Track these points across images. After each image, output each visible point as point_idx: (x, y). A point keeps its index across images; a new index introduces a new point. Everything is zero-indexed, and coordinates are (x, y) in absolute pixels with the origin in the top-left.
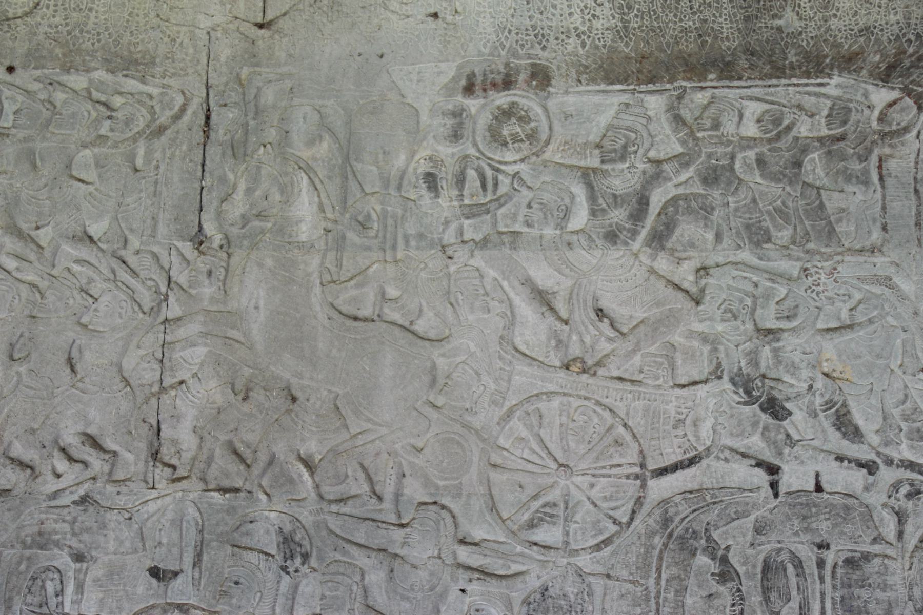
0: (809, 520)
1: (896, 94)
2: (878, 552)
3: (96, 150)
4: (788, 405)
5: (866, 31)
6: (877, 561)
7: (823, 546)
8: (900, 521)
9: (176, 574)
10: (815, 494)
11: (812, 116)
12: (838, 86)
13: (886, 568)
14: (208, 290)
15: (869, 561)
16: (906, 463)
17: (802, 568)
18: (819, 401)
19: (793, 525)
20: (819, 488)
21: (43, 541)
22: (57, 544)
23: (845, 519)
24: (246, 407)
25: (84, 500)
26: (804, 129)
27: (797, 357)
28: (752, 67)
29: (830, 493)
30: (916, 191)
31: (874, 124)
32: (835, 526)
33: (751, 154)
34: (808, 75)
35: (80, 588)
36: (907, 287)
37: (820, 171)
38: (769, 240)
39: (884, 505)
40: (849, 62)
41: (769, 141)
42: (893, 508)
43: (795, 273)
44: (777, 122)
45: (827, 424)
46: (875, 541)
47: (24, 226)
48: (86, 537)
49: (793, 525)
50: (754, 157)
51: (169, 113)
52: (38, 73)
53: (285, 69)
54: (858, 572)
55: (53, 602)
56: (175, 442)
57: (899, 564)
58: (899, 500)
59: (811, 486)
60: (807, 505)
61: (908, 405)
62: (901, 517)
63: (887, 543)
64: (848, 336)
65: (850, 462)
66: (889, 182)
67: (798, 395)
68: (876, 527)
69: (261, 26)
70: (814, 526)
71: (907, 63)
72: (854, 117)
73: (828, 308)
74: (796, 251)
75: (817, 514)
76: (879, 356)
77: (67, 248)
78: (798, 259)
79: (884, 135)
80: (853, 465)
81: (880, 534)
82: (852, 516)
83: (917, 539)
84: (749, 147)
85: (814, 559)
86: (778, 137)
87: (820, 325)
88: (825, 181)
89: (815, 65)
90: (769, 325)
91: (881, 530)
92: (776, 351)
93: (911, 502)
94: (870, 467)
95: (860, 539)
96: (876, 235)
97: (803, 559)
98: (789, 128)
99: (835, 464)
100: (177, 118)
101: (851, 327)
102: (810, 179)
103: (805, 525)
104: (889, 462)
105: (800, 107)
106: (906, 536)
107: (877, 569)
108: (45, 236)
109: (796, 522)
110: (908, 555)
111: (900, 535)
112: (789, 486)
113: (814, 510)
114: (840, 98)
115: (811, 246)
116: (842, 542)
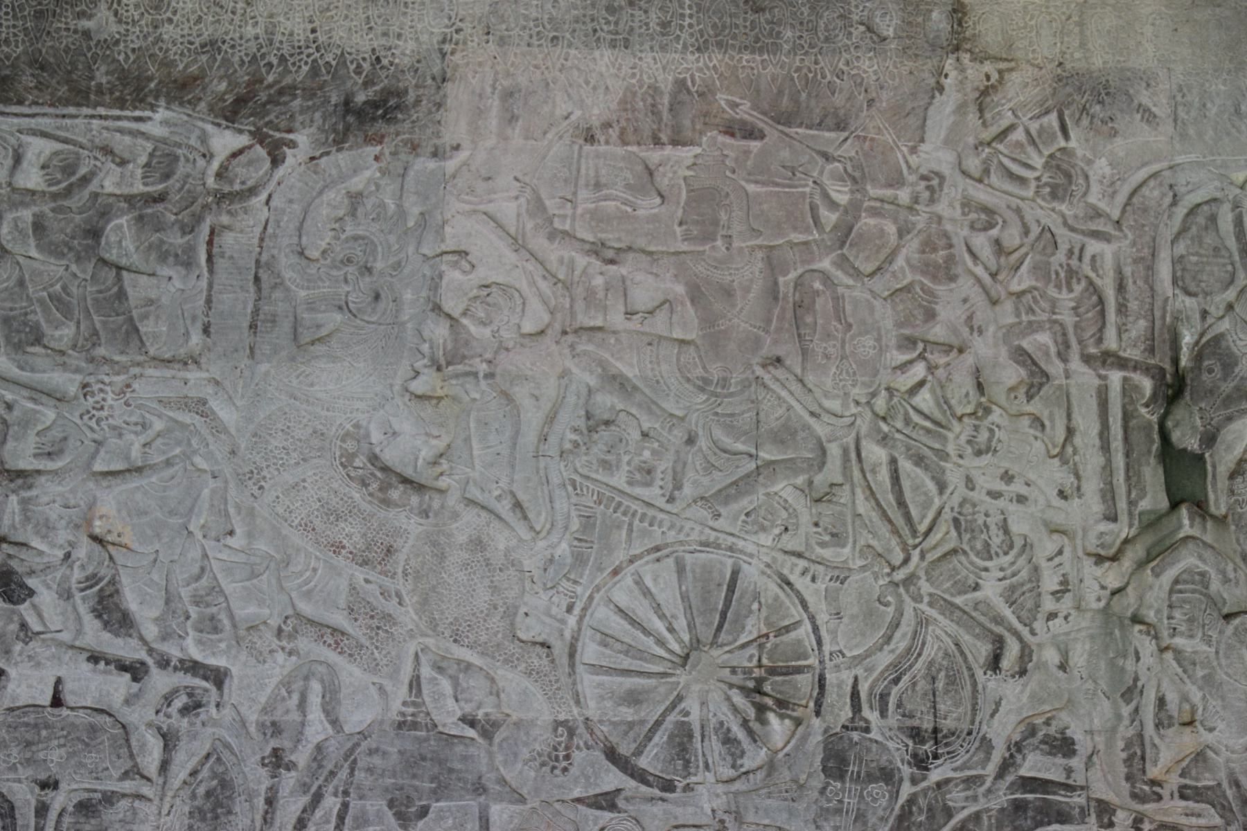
0: (34, 748)
1: (244, 140)
2: (128, 791)
4: (31, 582)
5: (212, 45)
6: (124, 804)
7: (49, 784)
8: (166, 746)
10: (49, 709)
11: (123, 163)
12: (165, 123)
13: (135, 814)
15: (112, 804)
16: (188, 664)
17: (13, 817)
18: (77, 574)
19: (9, 755)
20: (57, 702)
23: (87, 745)
26: (110, 182)
27: (54, 512)
28: (40, 86)
29: (72, 709)
30: (257, 279)
31: (211, 181)
32: (71, 755)
33: (27, 215)
34: (121, 103)
36: (226, 414)
37: (129, 244)
38: (38, 341)
39: (149, 725)
40: (182, 89)
41: (55, 196)
42: (159, 729)
43: (73, 389)
44: (69, 169)
45: (83, 609)
46: (126, 775)
49: (9, 755)
50: (30, 219)
54: (93, 821)
57: (154, 808)
58: (169, 716)
59: (46, 699)
60: (36, 725)
61: (204, 582)
62: (169, 740)
63: (143, 777)
64: (135, 482)
65: (107, 664)
66: (220, 264)
67: (48, 567)
68: (132, 756)
70: (41, 755)
71: (263, 96)
72: (182, 169)
73: (113, 442)
74: (75, 359)
75: (49, 739)
76: (172, 513)
78: (77, 370)
79: (221, 197)
80: (112, 667)
81: (136, 765)
82: (98, 741)
83: (188, 771)
84: (23, 204)
85: (33, 803)
86: (68, 192)
87: (98, 467)
88: (136, 260)
89: (133, 90)
90: (22, 465)
91: (139, 760)
92: (24, 502)
93: (186, 720)
94: (136, 671)
95: (106, 773)
96: (196, 338)
97: (17, 804)
98: (85, 180)
99: (86, 667)
101: (139, 470)
102: (112, 255)
103: (28, 755)
104: (164, 663)
105: (107, 151)
106: (174, 768)
107: (121, 816)
109: (15, 751)
110: (170, 794)
111: (164, 766)
112: (14, 699)
113: (44, 733)
114: (164, 141)
115: (101, 351)
116: (77, 778)
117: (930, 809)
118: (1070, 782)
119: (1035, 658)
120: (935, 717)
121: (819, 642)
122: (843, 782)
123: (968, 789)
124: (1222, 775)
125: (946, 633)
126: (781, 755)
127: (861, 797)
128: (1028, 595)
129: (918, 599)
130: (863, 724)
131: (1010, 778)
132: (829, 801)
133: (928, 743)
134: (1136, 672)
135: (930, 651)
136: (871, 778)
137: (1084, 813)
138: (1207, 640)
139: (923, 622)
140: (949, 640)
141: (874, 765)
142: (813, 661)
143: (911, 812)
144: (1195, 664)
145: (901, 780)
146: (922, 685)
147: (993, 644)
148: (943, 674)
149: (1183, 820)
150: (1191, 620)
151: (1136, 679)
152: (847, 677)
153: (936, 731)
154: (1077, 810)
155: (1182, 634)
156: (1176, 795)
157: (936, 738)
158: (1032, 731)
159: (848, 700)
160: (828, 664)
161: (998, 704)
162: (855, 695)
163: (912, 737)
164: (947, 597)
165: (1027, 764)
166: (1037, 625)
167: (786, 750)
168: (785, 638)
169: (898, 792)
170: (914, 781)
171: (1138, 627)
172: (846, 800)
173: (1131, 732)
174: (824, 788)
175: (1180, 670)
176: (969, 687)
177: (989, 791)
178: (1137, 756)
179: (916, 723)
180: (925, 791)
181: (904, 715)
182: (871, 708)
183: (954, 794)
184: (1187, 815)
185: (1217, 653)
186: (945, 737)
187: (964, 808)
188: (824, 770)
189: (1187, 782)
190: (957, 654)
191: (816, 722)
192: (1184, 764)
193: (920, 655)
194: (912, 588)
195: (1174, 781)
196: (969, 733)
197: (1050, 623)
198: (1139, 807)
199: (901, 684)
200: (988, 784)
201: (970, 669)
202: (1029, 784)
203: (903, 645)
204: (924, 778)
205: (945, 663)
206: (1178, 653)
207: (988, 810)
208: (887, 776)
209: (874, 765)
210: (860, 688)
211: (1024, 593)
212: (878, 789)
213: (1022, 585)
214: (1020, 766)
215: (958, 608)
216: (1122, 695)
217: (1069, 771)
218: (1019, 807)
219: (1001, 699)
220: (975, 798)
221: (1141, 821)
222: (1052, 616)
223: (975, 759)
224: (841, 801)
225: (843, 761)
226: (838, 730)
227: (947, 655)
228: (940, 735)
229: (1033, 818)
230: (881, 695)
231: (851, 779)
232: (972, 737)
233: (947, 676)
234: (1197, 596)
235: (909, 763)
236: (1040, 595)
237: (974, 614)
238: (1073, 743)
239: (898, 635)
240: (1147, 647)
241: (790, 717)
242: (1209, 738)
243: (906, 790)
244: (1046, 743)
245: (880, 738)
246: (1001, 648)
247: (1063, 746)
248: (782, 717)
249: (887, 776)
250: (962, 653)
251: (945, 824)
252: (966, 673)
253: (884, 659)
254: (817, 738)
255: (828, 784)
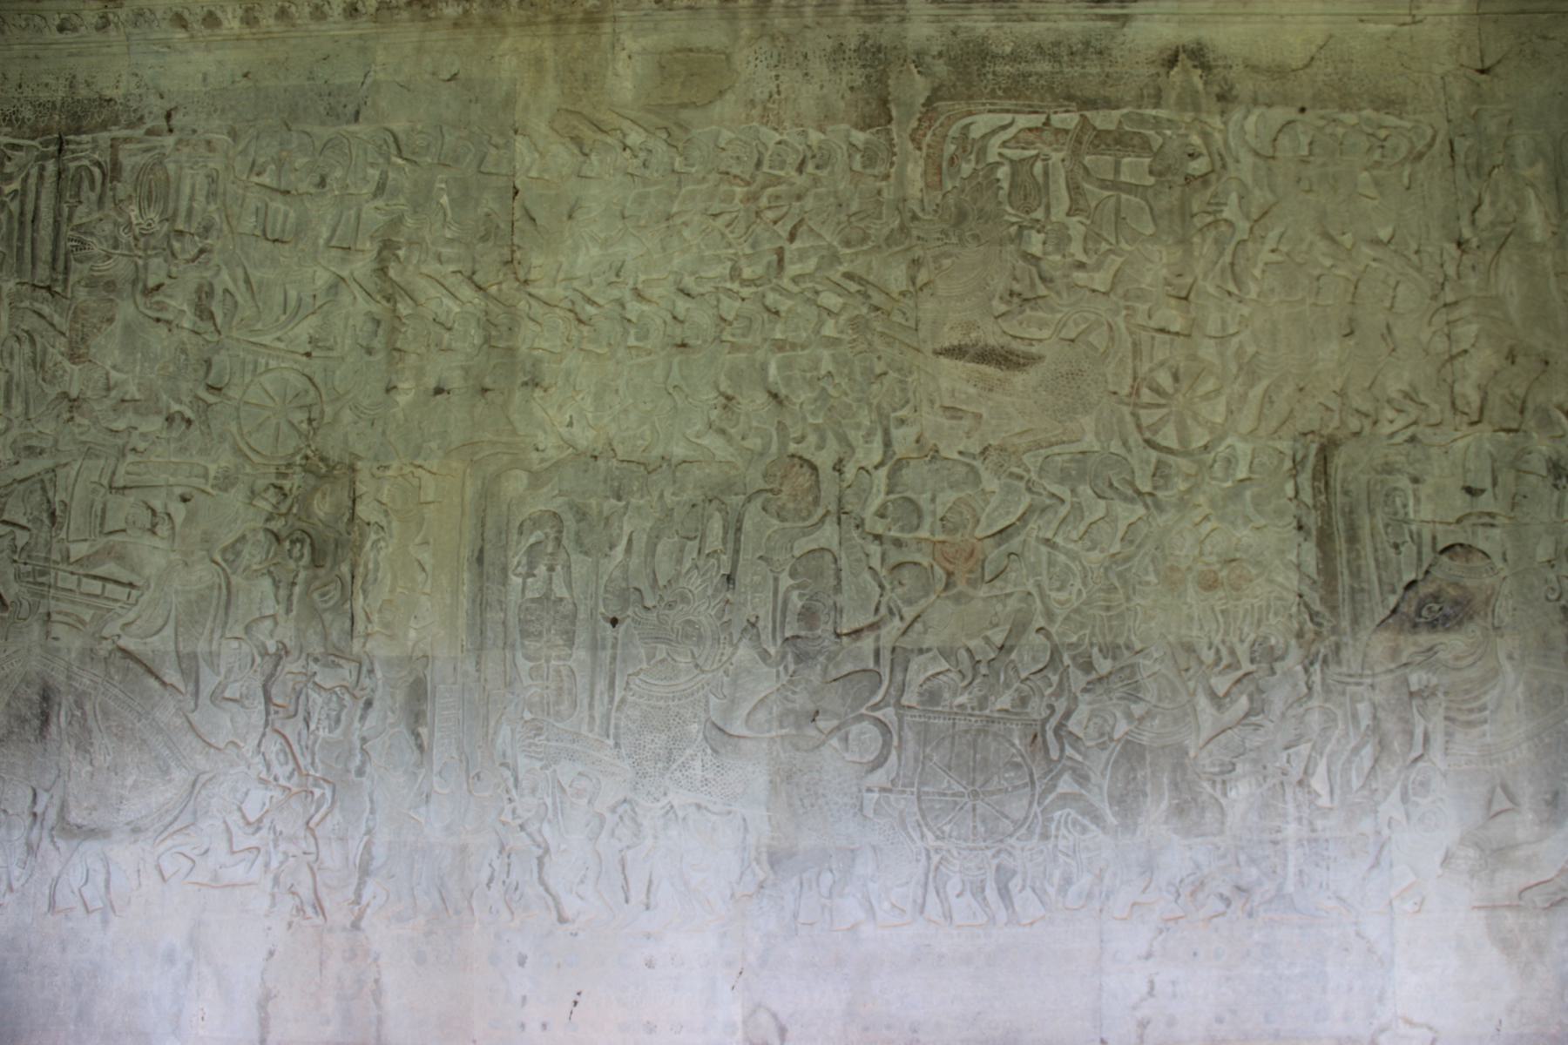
3: (1375, 172)
9: (1483, 491)
14: (1473, 281)
21: (1388, 469)
22: (1399, 470)
24: (1515, 369)
25: (1412, 439)
35: (1418, 500)
47: (1333, 233)
48: (1417, 466)
51: (1423, 142)
52: (1322, 112)
53: (1504, 106)
55: (1402, 512)
56: (1464, 396)
69: (1482, 72)
77: (1367, 250)
100: (1430, 145)
108: (1347, 240)
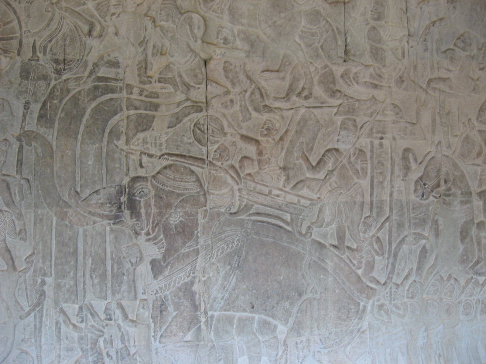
117: (61, 90)
118: (117, 78)
119: (105, 31)
120: (65, 54)
121: (21, 27)
122: (28, 81)
123: (76, 81)
124: (176, 73)
125: (71, 22)
126: (4, 71)
127: (35, 86)
128: (104, 6)
129: (60, 9)
130: (36, 58)
131: (93, 77)
132: (22, 88)
133: (62, 64)
134: (145, 35)
135: (65, 29)
136: (39, 79)
137: (121, 89)
138: (174, 22)
139: (62, 18)
140: (72, 25)
141: (40, 74)
142: (18, 35)
143: (54, 91)
144: (168, 32)
145: (51, 79)
146: (61, 42)
147: (89, 26)
148: (69, 38)
149: (159, 91)
150: (168, 15)
151: (145, 38)
152: (31, 40)
153: (64, 60)
154: (119, 88)
155: (164, 20)
156: (157, 81)
157: (64, 63)
158: (102, 58)
159: (31, 49)
160: (24, 35)
161: (91, 49)
162: (34, 47)
163: (55, 62)
164: (73, 8)
165: (101, 71)
166: (108, 18)
167: (6, 69)
168: (8, 26)
169: (49, 84)
170: (56, 80)
171: (147, 18)
172: (29, 88)
173: (142, 58)
174: (21, 84)
175: (162, 34)
176: (79, 43)
177: (85, 82)
178: (144, 67)
179: (57, 57)
180: (60, 83)
181: (53, 54)
182: (40, 52)
183: (71, 84)
184: (161, 88)
185: (177, 27)
186: (68, 62)
187: (74, 89)
188: (20, 76)
189: (162, 76)
190: (75, 30)
191: (18, 59)
192: (161, 70)
193: (60, 31)
194: (58, 5)
195: (157, 76)
196: (78, 60)
197: (112, 17)
198: (143, 86)
199: (52, 42)
200: (85, 79)
201: (79, 35)
202: (100, 79)
203: (54, 27)
204: (60, 78)
205: (70, 34)
206: (162, 28)
207: (83, 90)
208: (45, 78)
209: (40, 74)
210: (36, 44)
211: (103, 6)
212: (42, 83)
213: (102, 2)
214: (98, 72)
215: (77, 12)
216: (139, 44)
217: (118, 74)
218: (96, 88)
219: (92, 47)
220: (79, 85)
221: (143, 91)
222: (113, 14)
223: (80, 70)
224: (27, 88)
225: (28, 73)
226: (27, 61)
227: (71, 30)
228: (66, 62)
229: (101, 92)
230: (44, 47)
231: (31, 79)
232: (79, 62)
233: (70, 39)
234: (171, 5)
235: (54, 73)
236: (109, 6)
237: (83, 15)
238: (119, 63)
239: (52, 23)
240: (149, 24)
241: (9, 57)
242: (172, 60)
243: (53, 83)
244: (108, 63)
245: (43, 64)
246: (92, 27)
247: (115, 64)
248: (6, 57)
249: (45, 78)
250: (77, 30)
251: (67, 95)
252: (78, 37)
253: (47, 33)
254: (19, 64)
255: (22, 82)
